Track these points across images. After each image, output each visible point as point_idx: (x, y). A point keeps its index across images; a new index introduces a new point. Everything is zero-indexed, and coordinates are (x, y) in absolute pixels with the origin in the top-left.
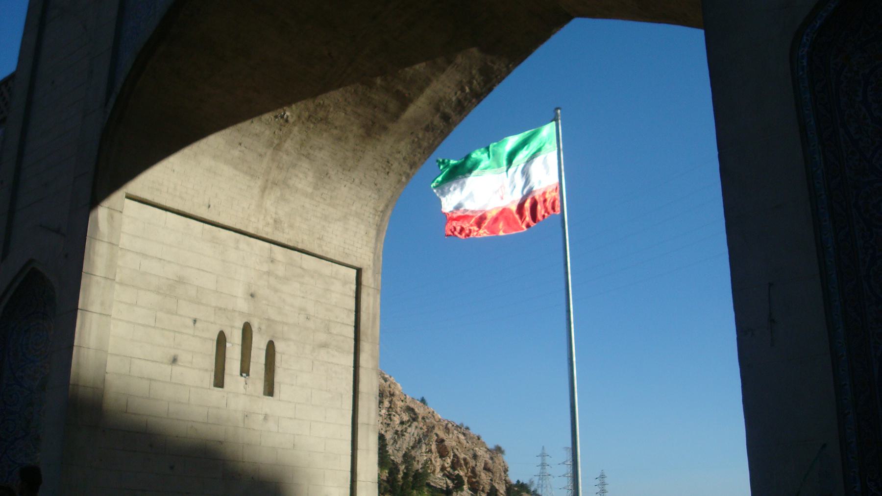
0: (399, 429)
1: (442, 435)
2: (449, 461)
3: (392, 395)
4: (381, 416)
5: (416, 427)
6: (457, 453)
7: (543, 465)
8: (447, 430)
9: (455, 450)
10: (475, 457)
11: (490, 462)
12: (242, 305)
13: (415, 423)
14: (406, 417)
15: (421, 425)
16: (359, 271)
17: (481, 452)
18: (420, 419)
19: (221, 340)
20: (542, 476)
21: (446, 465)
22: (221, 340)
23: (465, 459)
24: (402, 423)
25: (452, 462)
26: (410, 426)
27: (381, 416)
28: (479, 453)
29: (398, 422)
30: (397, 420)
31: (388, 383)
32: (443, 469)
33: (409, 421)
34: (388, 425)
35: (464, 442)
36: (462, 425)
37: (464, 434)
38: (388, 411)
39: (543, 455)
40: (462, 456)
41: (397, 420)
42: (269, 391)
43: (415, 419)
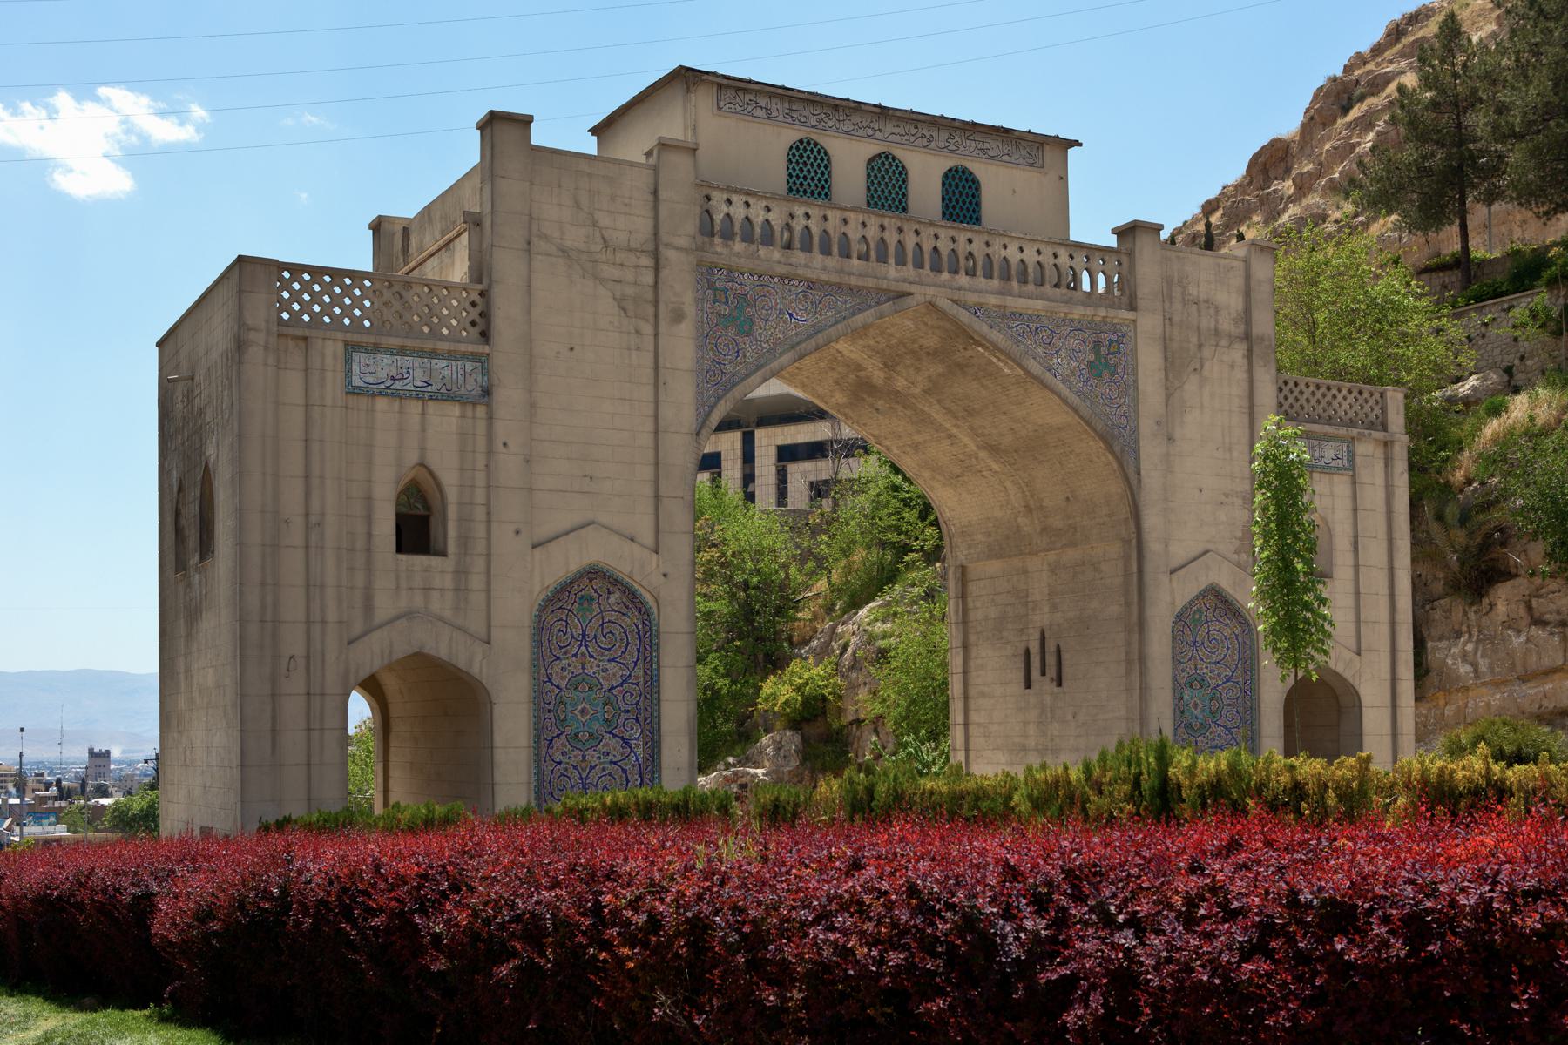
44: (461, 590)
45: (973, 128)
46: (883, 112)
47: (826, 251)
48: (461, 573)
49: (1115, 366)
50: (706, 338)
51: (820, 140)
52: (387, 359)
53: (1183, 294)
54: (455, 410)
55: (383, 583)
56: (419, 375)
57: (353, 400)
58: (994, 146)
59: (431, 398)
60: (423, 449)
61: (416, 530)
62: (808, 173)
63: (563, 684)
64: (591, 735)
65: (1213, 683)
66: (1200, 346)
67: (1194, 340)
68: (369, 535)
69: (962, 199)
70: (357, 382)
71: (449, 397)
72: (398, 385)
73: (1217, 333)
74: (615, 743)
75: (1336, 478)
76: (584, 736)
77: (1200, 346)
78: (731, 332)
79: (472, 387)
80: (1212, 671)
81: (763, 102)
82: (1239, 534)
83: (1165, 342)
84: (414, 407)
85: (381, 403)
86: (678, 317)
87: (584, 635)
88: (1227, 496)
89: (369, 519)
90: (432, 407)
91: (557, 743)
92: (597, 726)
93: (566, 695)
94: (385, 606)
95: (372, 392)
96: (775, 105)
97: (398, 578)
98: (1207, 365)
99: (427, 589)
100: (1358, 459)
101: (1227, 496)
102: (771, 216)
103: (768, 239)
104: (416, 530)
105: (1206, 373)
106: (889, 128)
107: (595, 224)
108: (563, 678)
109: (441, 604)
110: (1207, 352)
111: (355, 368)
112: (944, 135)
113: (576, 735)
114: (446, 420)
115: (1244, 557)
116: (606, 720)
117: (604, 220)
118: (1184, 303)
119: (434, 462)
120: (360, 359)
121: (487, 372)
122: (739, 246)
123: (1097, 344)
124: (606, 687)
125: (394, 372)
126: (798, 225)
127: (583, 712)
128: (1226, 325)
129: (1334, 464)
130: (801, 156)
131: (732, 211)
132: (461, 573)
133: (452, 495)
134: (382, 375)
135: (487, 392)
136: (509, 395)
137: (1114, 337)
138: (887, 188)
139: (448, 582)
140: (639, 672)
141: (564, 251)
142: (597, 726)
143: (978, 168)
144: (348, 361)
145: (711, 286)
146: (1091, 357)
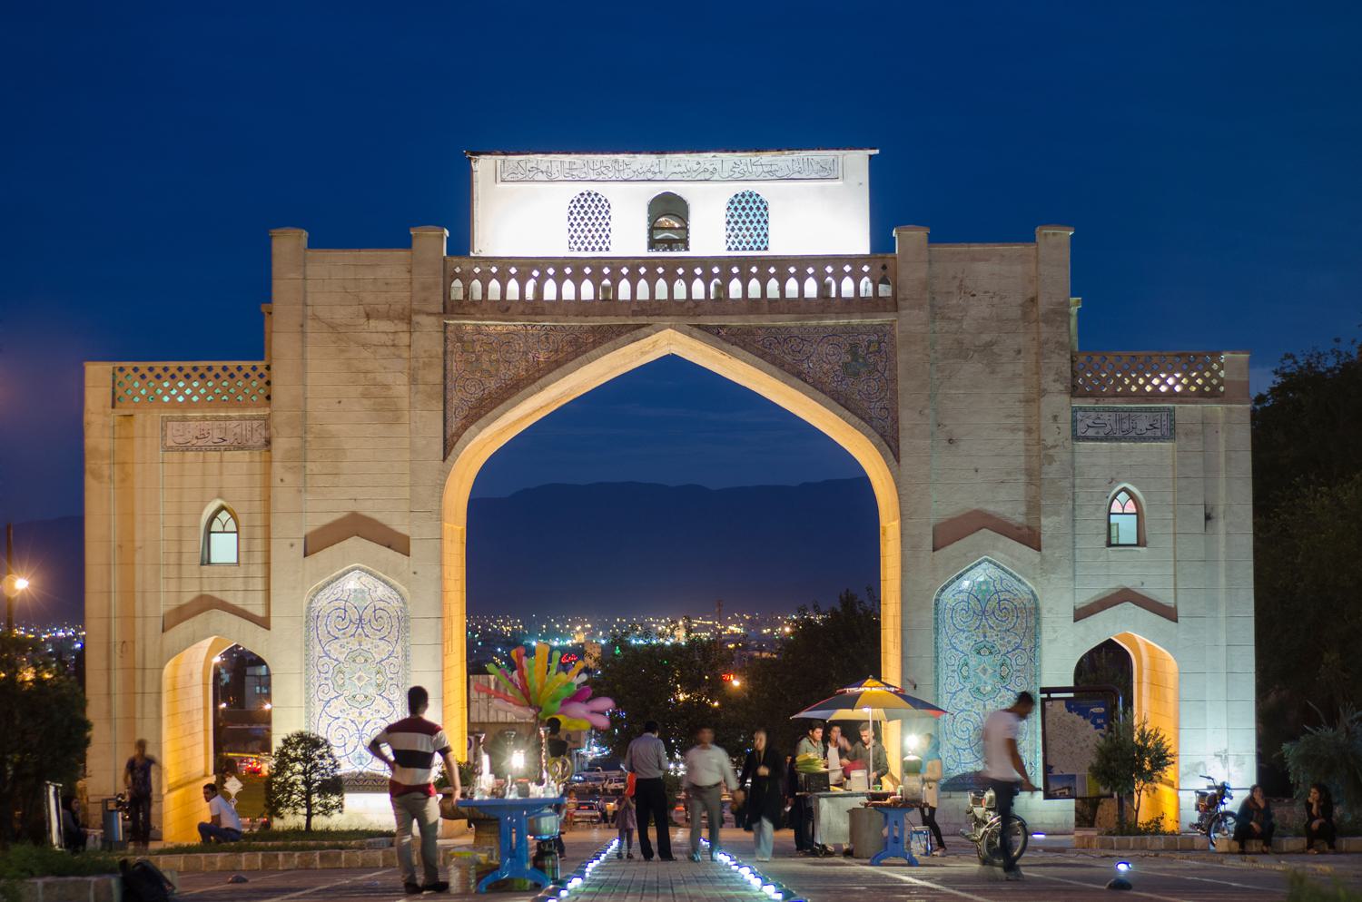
49: (875, 364)
56: (216, 435)
59: (225, 450)
63: (342, 658)
64: (366, 697)
65: (1004, 650)
68: (180, 553)
70: (170, 443)
72: (200, 443)
74: (384, 703)
76: (360, 698)
79: (258, 439)
80: (1002, 639)
87: (360, 619)
88: (1008, 474)
97: (201, 583)
101: (1008, 474)
108: (341, 653)
111: (169, 433)
113: (354, 697)
116: (378, 685)
120: (172, 425)
121: (267, 428)
124: (378, 660)
125: (198, 434)
127: (359, 679)
129: (1149, 434)
130: (582, 207)
134: (189, 437)
135: (268, 442)
137: (874, 338)
140: (398, 648)
143: (764, 189)
146: (848, 358)
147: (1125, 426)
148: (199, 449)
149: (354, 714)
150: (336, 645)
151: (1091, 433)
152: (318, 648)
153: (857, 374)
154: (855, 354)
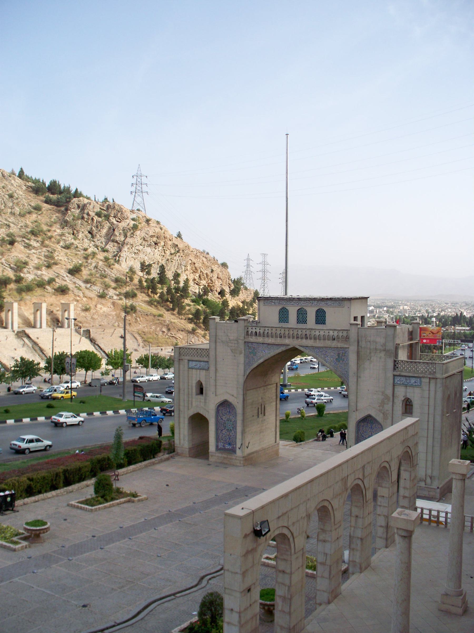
0: (169, 258)
1: (194, 260)
2: (198, 275)
3: (165, 238)
4: (159, 251)
5: (179, 256)
6: (202, 270)
7: (248, 266)
8: (196, 256)
9: (201, 269)
10: (212, 271)
11: (221, 274)
12: (261, 401)
13: (178, 254)
14: (173, 251)
15: (182, 255)
16: (277, 384)
17: (215, 268)
18: (181, 251)
19: (258, 408)
20: (248, 272)
21: (196, 278)
22: (258, 408)
23: (207, 274)
24: (171, 254)
25: (200, 276)
26: (175, 256)
27: (159, 251)
28: (214, 269)
29: (169, 254)
30: (168, 253)
31: (163, 231)
32: (194, 280)
33: (174, 253)
34: (163, 256)
35: (206, 263)
36: (204, 251)
37: (206, 258)
38: (163, 248)
39: (248, 260)
40: (205, 272)
41: (168, 253)
42: (264, 415)
43: (178, 252)
44: (205, 402)
45: (323, 300)
46: (299, 299)
47: (272, 337)
48: (205, 399)
50: (246, 357)
51: (287, 308)
52: (194, 362)
53: (366, 339)
54: (204, 371)
55: (194, 400)
56: (199, 365)
57: (190, 370)
58: (329, 303)
60: (200, 378)
61: (201, 391)
62: (284, 316)
66: (370, 353)
67: (368, 351)
69: (321, 317)
71: (203, 369)
73: (376, 349)
75: (415, 388)
77: (370, 353)
78: (252, 355)
79: (206, 367)
81: (273, 301)
82: (380, 402)
83: (358, 353)
84: (198, 371)
85: (194, 370)
86: (241, 353)
89: (192, 389)
90: (201, 371)
91: (223, 431)
92: (232, 429)
93: (226, 422)
94: (194, 404)
95: (192, 368)
96: (276, 301)
98: (372, 358)
99: (200, 402)
100: (423, 383)
102: (261, 331)
103: (260, 335)
104: (201, 391)
105: (372, 360)
106: (302, 302)
107: (228, 336)
109: (202, 404)
110: (372, 354)
112: (316, 302)
114: (203, 373)
115: (381, 408)
117: (229, 335)
118: (366, 342)
119: (201, 380)
120: (190, 362)
122: (254, 337)
123: (339, 354)
126: (266, 332)
128: (379, 347)
131: (253, 330)
132: (205, 399)
133: (204, 386)
135: (209, 368)
136: (212, 368)
138: (302, 317)
139: (203, 401)
141: (222, 341)
142: (232, 429)
144: (188, 363)
145: (248, 346)
146: (337, 357)
147: (408, 381)
148: (196, 369)
149: (228, 433)
150: (224, 417)
151: (399, 382)
152: (219, 417)
153: (339, 362)
154: (339, 356)
